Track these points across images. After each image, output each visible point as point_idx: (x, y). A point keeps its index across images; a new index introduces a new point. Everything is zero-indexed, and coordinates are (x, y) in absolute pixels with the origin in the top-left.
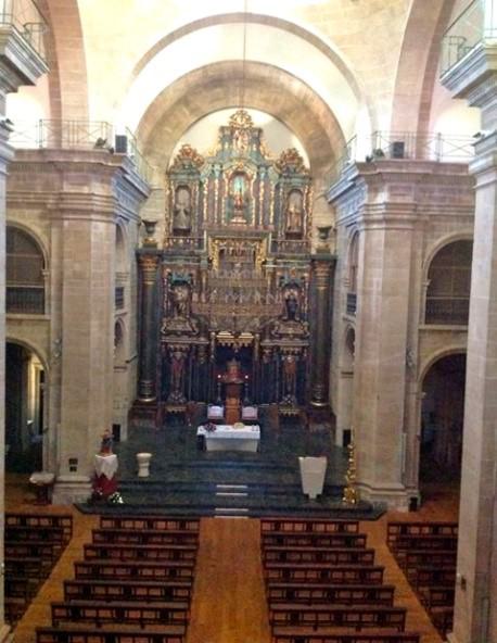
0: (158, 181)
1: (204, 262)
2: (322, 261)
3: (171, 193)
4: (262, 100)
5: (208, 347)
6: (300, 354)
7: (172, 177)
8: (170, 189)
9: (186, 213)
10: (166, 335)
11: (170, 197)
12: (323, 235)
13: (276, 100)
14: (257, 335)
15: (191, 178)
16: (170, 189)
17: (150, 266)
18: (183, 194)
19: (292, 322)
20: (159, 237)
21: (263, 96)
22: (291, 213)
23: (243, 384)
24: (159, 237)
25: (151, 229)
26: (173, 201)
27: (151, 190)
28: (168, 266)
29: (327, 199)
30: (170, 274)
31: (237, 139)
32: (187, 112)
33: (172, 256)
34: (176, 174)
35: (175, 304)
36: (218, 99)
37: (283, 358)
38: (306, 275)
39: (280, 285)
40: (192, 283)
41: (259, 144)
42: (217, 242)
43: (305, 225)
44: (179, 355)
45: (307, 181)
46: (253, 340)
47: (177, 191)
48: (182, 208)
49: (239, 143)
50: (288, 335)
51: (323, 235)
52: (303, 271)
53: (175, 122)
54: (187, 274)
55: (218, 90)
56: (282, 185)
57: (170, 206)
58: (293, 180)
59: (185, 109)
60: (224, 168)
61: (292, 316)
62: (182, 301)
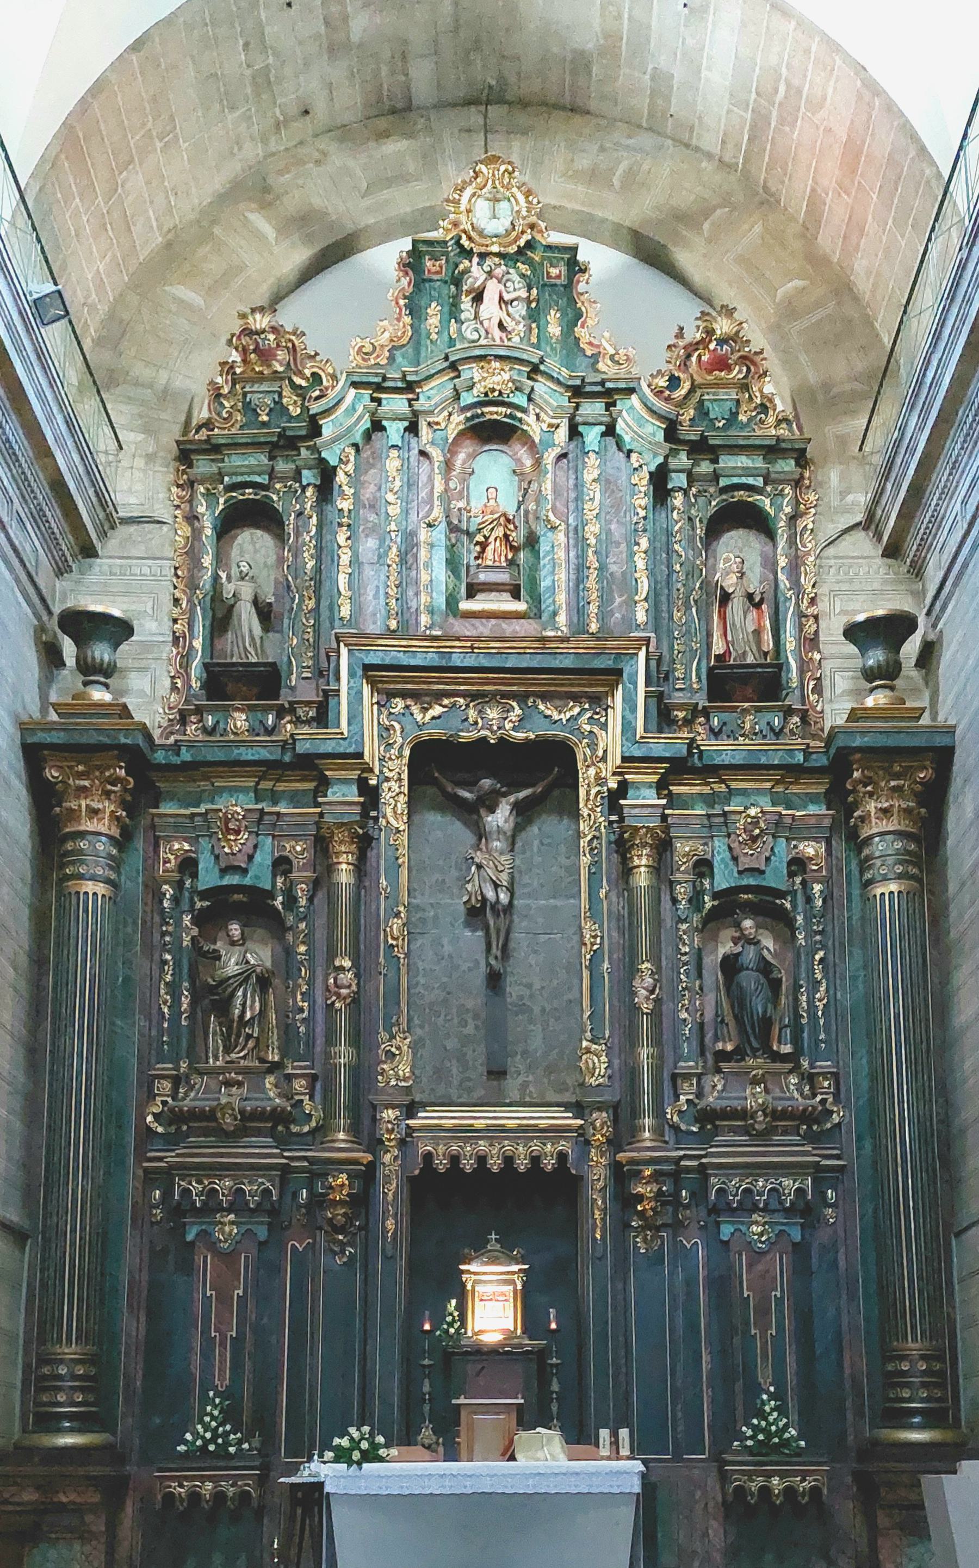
0: (140, 482)
1: (343, 794)
2: (886, 757)
3: (197, 534)
4: (576, 176)
5: (367, 1176)
6: (805, 1210)
7: (203, 466)
8: (192, 518)
9: (265, 613)
10: (171, 1141)
11: (192, 554)
12: (876, 656)
13: (630, 174)
14: (600, 1117)
15: (282, 466)
16: (192, 518)
17: (96, 819)
18: (252, 545)
19: (756, 1064)
20: (149, 690)
21: (583, 162)
22: (726, 598)
23: (541, 1355)
24: (149, 690)
25: (101, 652)
26: (207, 561)
27: (110, 521)
28: (182, 827)
29: (878, 536)
30: (188, 865)
31: (478, 298)
32: (268, 230)
33: (199, 771)
34: (214, 449)
35: (214, 999)
36: (402, 178)
37: (726, 1231)
38: (809, 849)
39: (695, 901)
40: (290, 901)
41: (574, 317)
42: (399, 704)
43: (790, 643)
44: (227, 1228)
45: (787, 466)
46: (583, 1140)
47: (228, 524)
48: (247, 591)
49: (490, 308)
50: (743, 1114)
51: (876, 656)
52: (795, 831)
53: (214, 266)
54: (264, 858)
55: (394, 147)
56: (678, 480)
57: (193, 586)
58: (727, 462)
59: (259, 221)
60: (420, 405)
61: (756, 1034)
62: (244, 978)
